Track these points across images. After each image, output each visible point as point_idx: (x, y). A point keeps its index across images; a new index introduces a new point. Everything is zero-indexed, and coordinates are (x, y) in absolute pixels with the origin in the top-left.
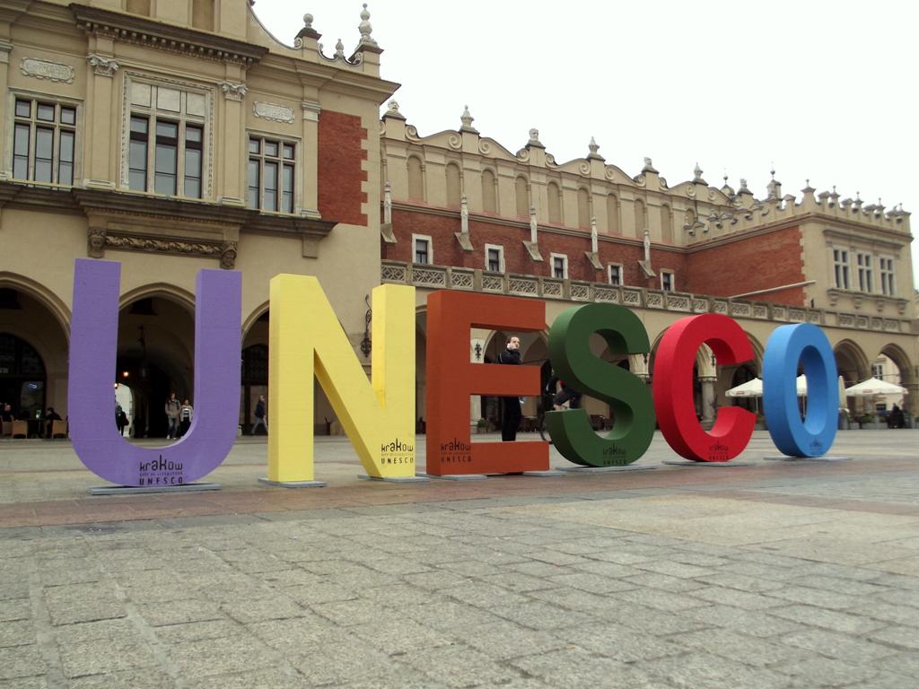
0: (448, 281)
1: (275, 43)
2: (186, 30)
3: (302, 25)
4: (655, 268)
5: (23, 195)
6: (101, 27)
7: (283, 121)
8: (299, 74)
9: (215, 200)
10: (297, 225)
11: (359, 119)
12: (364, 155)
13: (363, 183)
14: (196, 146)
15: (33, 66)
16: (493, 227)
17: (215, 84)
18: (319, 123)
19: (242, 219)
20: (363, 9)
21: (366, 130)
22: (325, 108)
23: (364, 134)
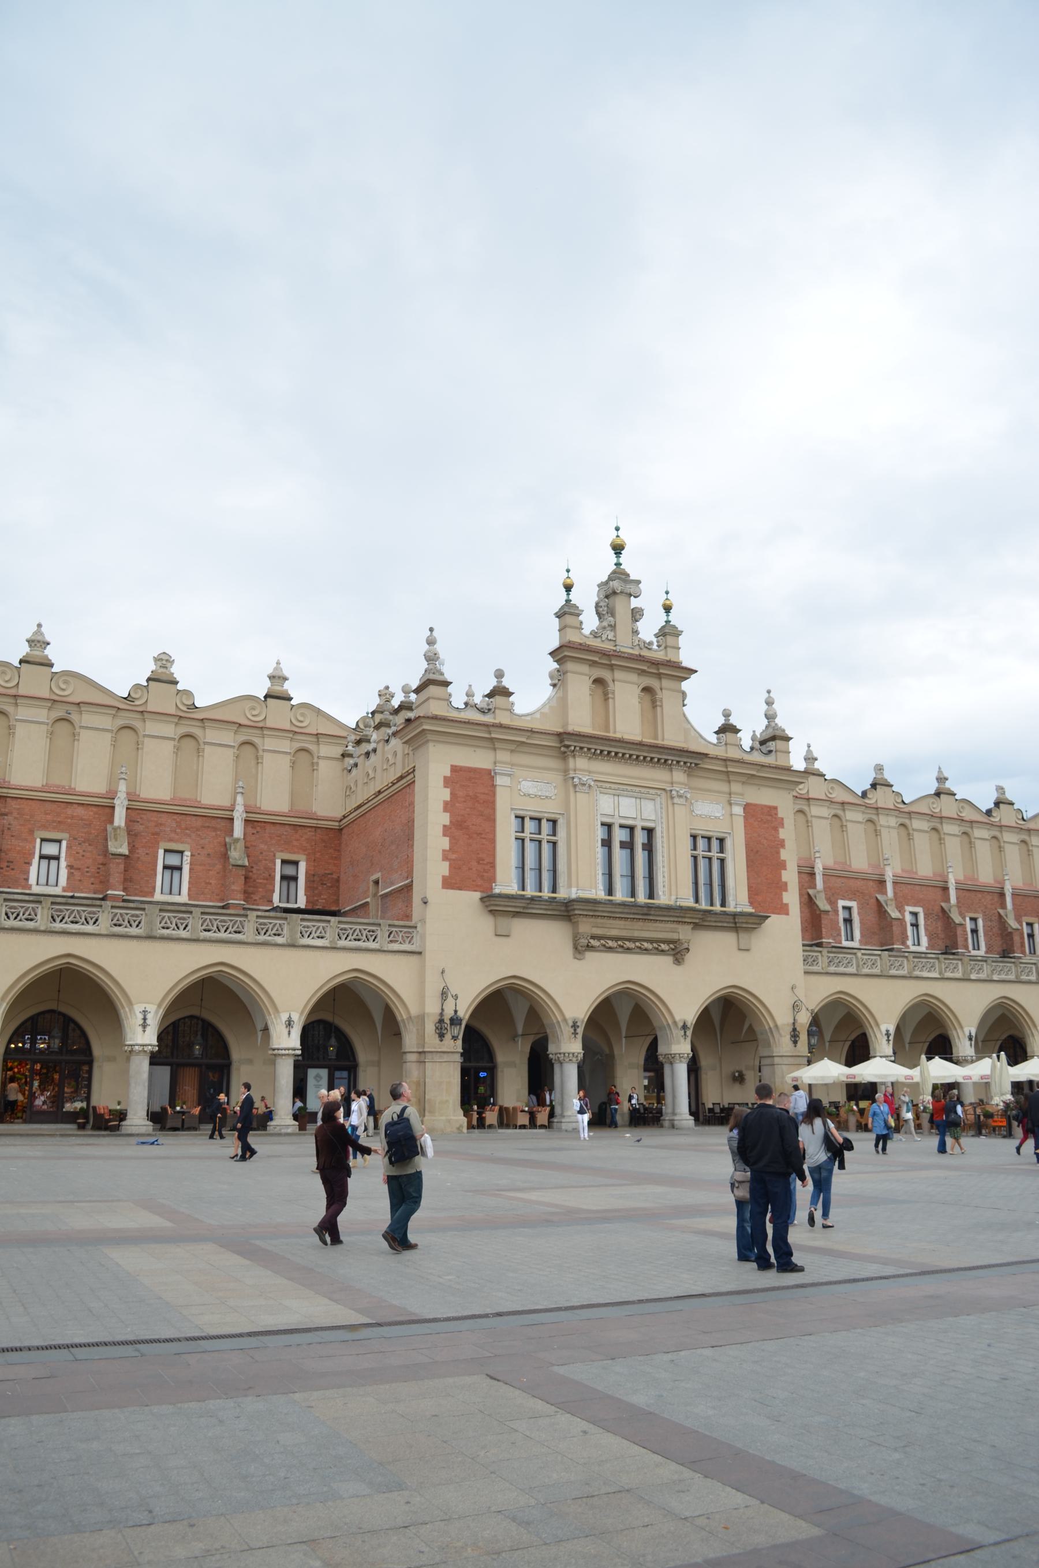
0: (858, 966)
1: (703, 741)
2: (641, 744)
3: (721, 721)
4: (1019, 920)
5: (530, 906)
6: (581, 748)
7: (716, 817)
8: (728, 772)
9: (670, 900)
10: (737, 920)
11: (776, 808)
12: (782, 844)
13: (783, 872)
14: (649, 847)
15: (527, 786)
16: (843, 880)
17: (664, 789)
18: (744, 817)
19: (696, 918)
20: (767, 695)
21: (782, 819)
22: (749, 801)
23: (781, 823)
